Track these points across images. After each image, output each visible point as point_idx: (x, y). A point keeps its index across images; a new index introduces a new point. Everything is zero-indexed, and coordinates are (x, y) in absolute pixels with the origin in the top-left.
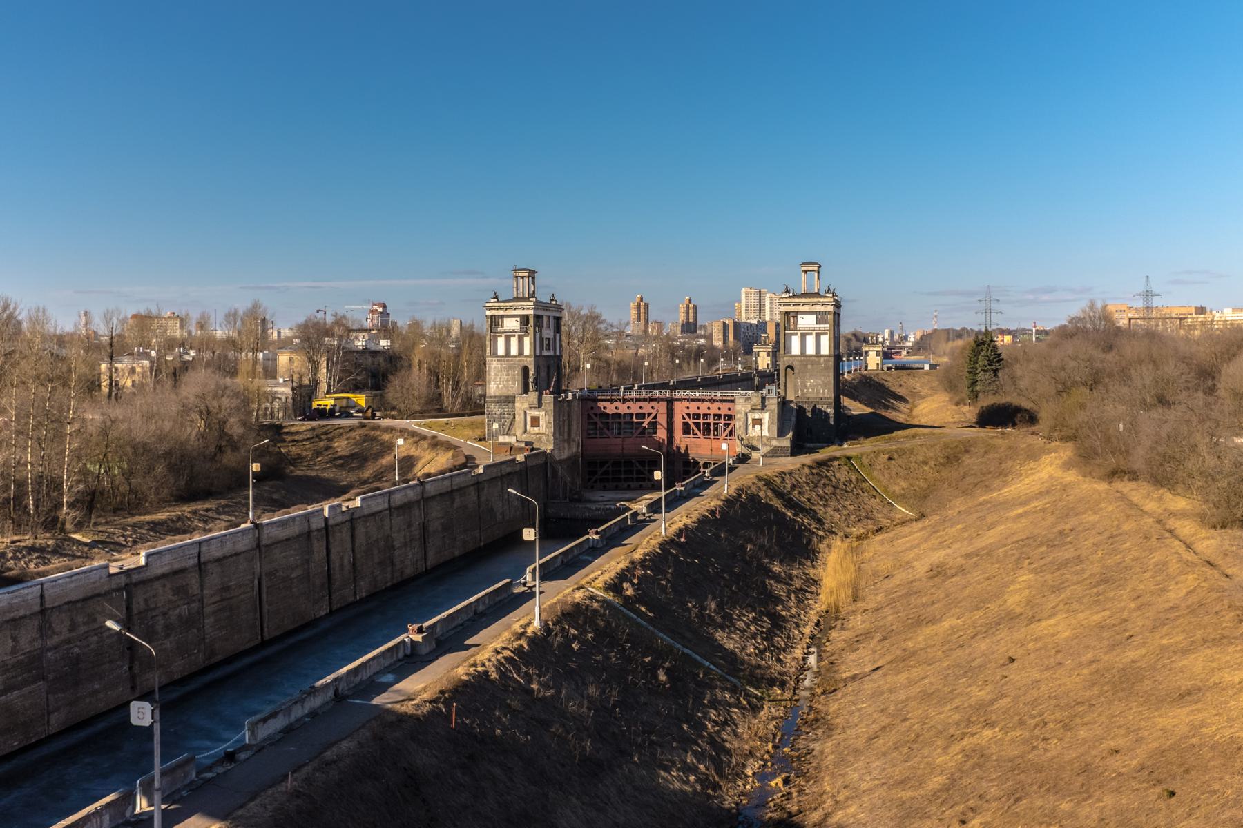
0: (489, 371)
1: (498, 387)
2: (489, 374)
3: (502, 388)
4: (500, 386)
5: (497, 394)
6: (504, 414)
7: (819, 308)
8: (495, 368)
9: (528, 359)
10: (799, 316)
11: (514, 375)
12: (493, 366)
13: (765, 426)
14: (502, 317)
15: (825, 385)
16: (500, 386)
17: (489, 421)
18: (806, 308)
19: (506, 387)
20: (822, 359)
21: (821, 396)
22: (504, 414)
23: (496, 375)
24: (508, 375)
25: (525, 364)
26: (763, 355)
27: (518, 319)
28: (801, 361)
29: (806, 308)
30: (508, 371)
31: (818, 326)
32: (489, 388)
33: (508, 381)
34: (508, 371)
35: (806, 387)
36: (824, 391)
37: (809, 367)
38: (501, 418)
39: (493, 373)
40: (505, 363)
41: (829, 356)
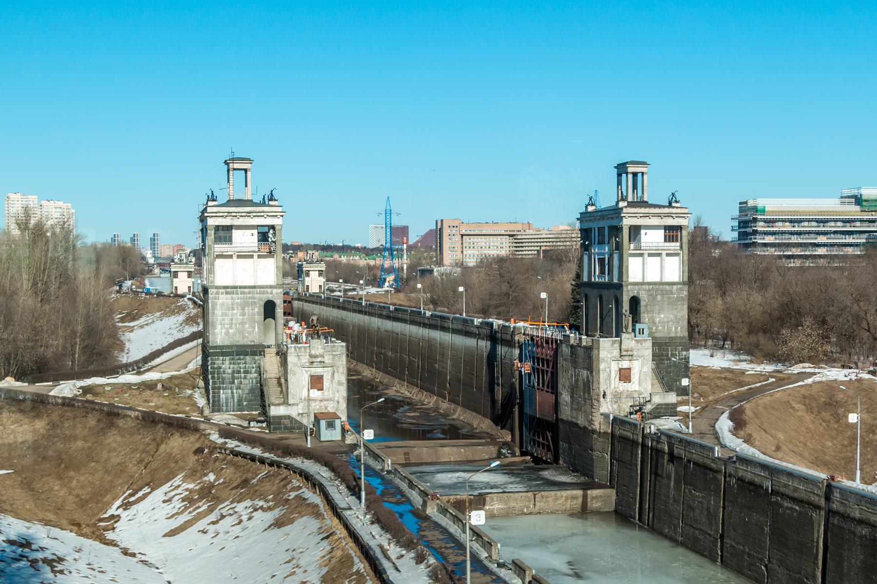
0: (214, 309)
1: (227, 333)
2: (213, 313)
3: (234, 334)
4: (231, 331)
5: (227, 343)
6: (239, 372)
7: (670, 222)
8: (223, 304)
9: (275, 291)
10: (643, 232)
11: (253, 314)
12: (219, 302)
13: (635, 377)
14: (229, 228)
15: (677, 320)
16: (231, 331)
17: (214, 383)
18: (655, 221)
19: (241, 333)
20: (675, 287)
21: (673, 335)
22: (239, 372)
23: (224, 314)
24: (243, 314)
25: (270, 297)
26: (314, 275)
27: (255, 232)
28: (649, 290)
29: (655, 221)
30: (243, 309)
31: (668, 244)
32: (214, 334)
33: (243, 323)
34: (243, 309)
35: (654, 323)
36: (676, 328)
37: (659, 298)
38: (233, 378)
39: (218, 312)
40: (238, 298)
41: (684, 283)
